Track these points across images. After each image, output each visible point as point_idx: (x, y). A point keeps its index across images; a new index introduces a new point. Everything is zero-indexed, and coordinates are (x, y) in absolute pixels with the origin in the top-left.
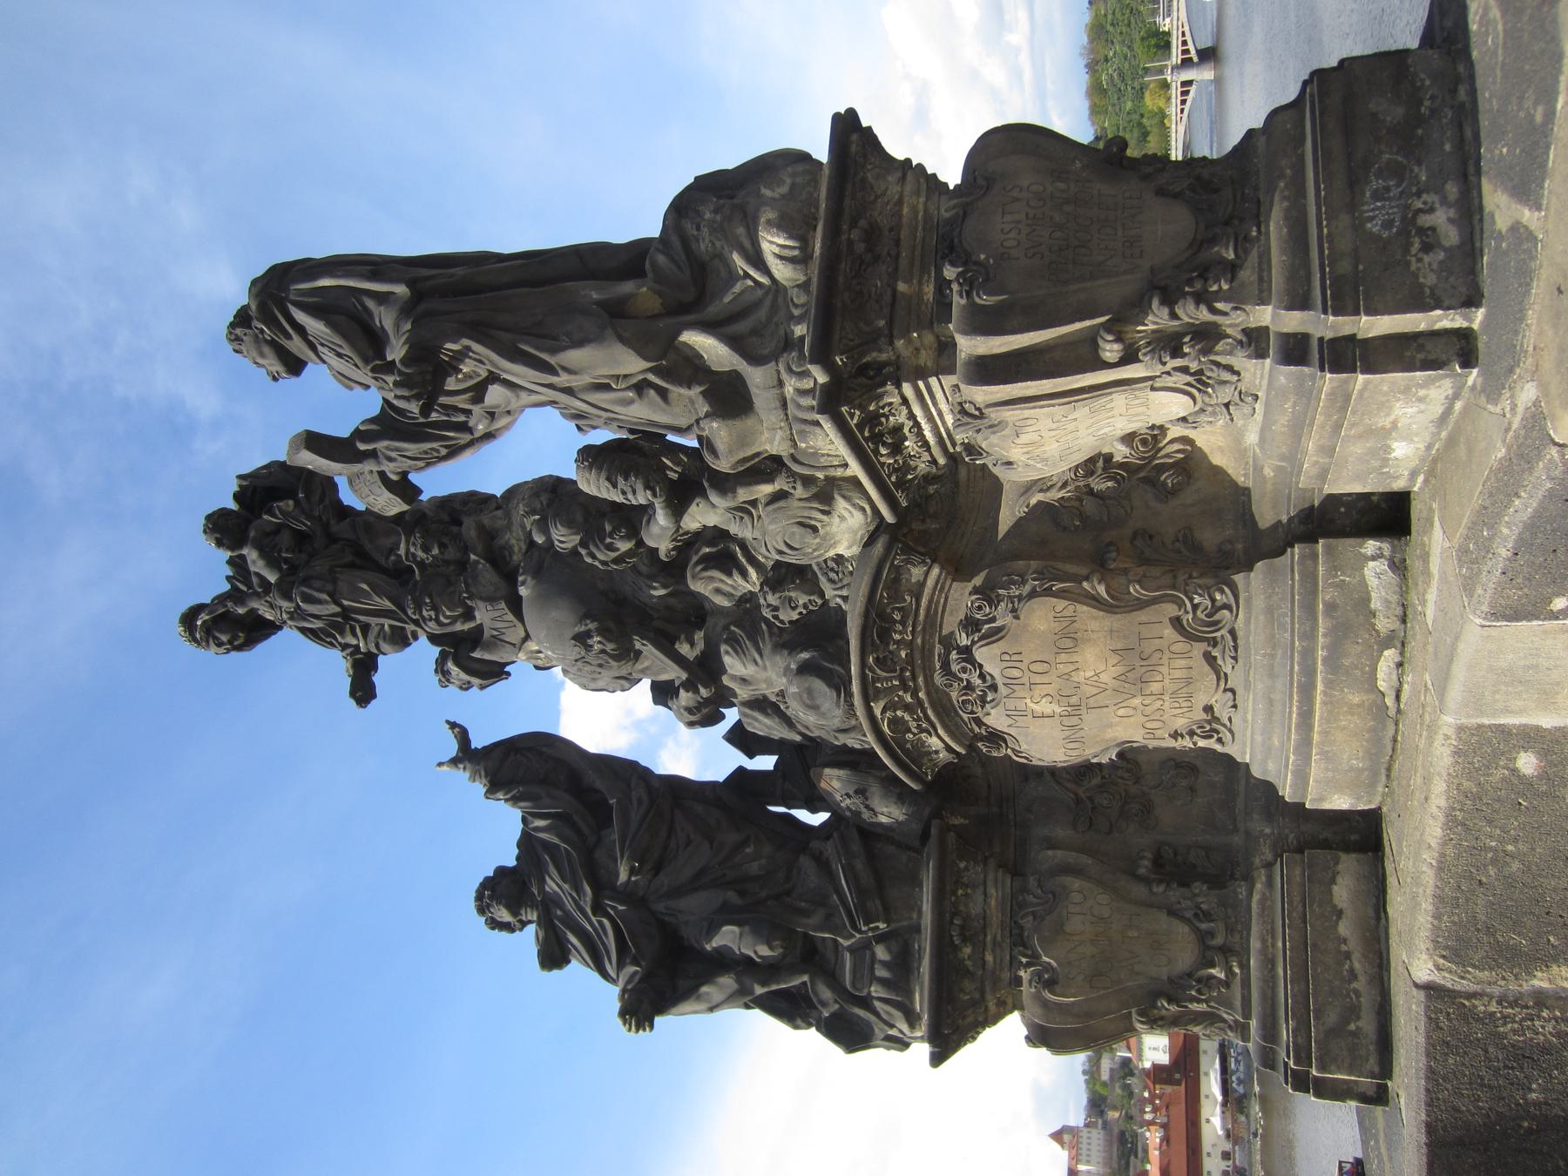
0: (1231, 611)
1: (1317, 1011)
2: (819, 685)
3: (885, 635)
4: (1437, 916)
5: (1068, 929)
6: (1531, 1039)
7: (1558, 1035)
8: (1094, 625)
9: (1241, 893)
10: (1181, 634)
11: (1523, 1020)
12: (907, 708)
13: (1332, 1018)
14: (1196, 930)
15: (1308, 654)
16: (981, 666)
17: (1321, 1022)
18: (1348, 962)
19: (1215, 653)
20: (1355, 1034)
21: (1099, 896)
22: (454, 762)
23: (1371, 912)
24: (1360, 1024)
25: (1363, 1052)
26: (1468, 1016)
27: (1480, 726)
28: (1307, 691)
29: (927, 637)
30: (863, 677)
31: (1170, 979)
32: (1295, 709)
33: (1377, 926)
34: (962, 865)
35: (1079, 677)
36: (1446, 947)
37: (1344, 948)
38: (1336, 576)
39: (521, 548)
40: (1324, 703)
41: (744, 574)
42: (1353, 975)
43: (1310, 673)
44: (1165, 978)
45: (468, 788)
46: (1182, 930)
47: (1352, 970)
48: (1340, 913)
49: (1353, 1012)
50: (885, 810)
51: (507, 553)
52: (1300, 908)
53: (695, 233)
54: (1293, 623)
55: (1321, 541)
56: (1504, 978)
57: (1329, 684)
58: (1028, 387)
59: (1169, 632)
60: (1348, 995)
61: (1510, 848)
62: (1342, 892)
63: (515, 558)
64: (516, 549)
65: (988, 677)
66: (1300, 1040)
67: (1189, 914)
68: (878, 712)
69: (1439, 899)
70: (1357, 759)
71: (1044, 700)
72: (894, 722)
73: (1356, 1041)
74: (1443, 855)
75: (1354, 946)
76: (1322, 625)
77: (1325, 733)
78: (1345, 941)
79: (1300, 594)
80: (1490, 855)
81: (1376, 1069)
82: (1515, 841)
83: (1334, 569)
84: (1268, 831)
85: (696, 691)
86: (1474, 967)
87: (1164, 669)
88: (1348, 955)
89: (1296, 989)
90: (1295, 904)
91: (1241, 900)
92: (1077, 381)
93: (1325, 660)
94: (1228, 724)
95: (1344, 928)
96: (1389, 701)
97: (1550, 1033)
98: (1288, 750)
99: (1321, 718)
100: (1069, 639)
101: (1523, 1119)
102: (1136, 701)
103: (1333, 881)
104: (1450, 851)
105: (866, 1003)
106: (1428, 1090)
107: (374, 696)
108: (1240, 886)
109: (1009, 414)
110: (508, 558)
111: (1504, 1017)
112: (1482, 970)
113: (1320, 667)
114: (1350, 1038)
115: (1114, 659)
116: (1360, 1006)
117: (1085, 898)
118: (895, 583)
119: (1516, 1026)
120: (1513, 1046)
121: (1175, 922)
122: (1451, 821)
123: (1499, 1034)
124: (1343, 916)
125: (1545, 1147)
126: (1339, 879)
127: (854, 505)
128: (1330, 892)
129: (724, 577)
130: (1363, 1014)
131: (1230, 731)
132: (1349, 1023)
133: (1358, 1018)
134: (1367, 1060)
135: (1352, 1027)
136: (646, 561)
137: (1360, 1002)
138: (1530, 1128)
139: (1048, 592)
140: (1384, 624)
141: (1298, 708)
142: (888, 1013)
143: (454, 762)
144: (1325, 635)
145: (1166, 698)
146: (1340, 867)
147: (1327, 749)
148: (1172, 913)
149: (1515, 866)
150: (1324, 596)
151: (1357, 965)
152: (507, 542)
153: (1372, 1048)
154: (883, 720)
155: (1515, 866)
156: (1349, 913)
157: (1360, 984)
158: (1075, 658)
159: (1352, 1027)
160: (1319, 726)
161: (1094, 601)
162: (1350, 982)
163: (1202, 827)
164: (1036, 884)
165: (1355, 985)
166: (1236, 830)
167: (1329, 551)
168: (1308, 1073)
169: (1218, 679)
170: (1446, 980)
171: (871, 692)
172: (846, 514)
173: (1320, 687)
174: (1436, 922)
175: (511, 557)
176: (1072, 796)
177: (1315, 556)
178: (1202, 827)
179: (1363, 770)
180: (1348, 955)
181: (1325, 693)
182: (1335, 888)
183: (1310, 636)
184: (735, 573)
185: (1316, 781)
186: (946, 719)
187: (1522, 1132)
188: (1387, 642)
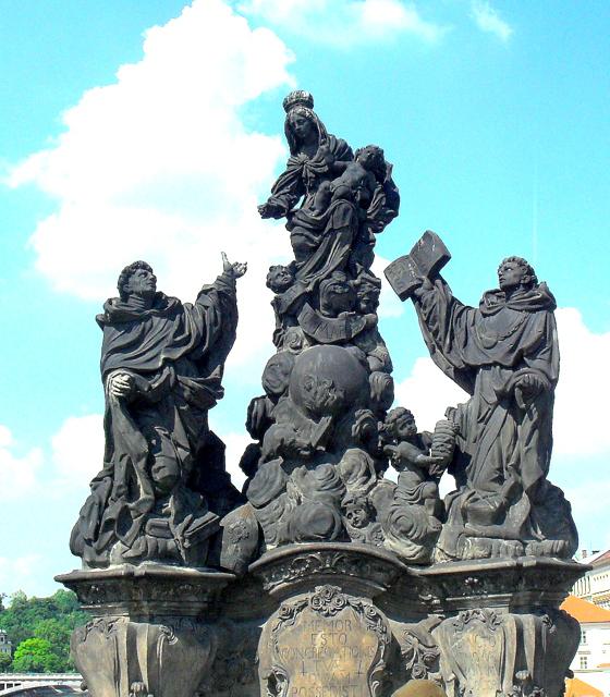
2: (327, 527)
3: (355, 562)
30: (336, 550)
35: (336, 657)
41: (364, 483)
45: (211, 274)
58: (512, 643)
85: (305, 449)
92: (511, 662)
100: (358, 655)
105: (142, 531)
109: (499, 637)
129: (362, 472)
139: (380, 644)
142: (139, 546)
158: (347, 657)
161: (373, 666)
172: (412, 548)
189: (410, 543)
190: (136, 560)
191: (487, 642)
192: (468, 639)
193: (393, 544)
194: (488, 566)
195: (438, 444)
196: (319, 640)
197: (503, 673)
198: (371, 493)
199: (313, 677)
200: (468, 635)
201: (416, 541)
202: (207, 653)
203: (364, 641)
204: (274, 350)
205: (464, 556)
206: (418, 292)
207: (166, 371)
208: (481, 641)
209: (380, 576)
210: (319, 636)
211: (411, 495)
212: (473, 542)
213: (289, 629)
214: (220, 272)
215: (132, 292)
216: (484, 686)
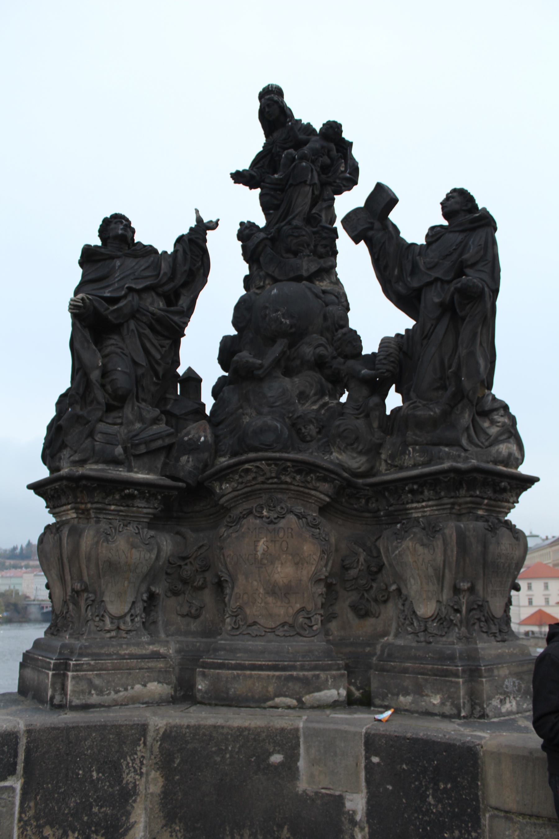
0: (308, 634)
1: (100, 674)
3: (299, 472)
4: (188, 727)
5: (134, 551)
6: (124, 772)
7: (127, 784)
8: (305, 572)
9: (144, 638)
10: (297, 611)
11: (134, 768)
12: (254, 478)
13: (97, 681)
14: (125, 615)
15: (294, 668)
16: (283, 518)
17: (95, 677)
18: (123, 690)
19: (286, 628)
20: (90, 693)
21: (146, 567)
22: (199, 220)
23: (146, 700)
24: (95, 696)
25: (81, 697)
26: (136, 743)
27: (298, 738)
28: (275, 668)
29: (293, 492)
31: (103, 601)
32: (264, 663)
33: (139, 703)
34: (159, 497)
36: (171, 732)
37: (129, 688)
38: (331, 678)
39: (322, 286)
40: (268, 676)
42: (117, 692)
43: (284, 669)
44: (104, 599)
46: (126, 609)
47: (119, 691)
48: (145, 685)
49: (100, 692)
50: (191, 459)
51: (320, 278)
52: (146, 667)
53: (500, 414)
54: (308, 661)
55: (346, 672)
56: (155, 758)
57: (279, 677)
59: (298, 606)
60: (108, 690)
61: (228, 756)
62: (154, 686)
63: (317, 283)
64: (321, 284)
65: (276, 521)
66: (85, 666)
67: (133, 611)
68: (258, 464)
69: (197, 728)
70: (235, 691)
71: (265, 547)
72: (247, 471)
73: (87, 694)
74: (223, 727)
75: (130, 692)
76: (309, 674)
77: (251, 676)
78: (132, 688)
79: (322, 664)
80: (224, 748)
81: (73, 704)
82: (231, 757)
83: (334, 677)
84: (171, 651)
86: (160, 745)
87: (279, 603)
88: (126, 689)
89: (109, 665)
90: (148, 664)
91: (141, 638)
93: (291, 676)
94: (245, 632)
95: (138, 687)
96: (270, 703)
97: (128, 780)
98: (236, 660)
99: (260, 675)
101: (84, 771)
102: (261, 591)
103: (159, 682)
104: (225, 731)
106: (95, 726)
107: (235, 182)
108: (147, 637)
110: (317, 279)
111: (134, 759)
112: (159, 748)
113: (288, 673)
114: (87, 691)
115: (285, 581)
116: (103, 695)
117: (147, 560)
118: (324, 479)
119: (130, 765)
120: (121, 764)
121: (130, 606)
122: (241, 730)
123: (126, 757)
124: (143, 687)
125: (70, 782)
126: (160, 685)
127: (363, 464)
128: (154, 681)
130: (99, 697)
131: (240, 634)
132: (95, 690)
133: (97, 695)
134: (78, 699)
135: (93, 692)
136: (321, 352)
137: (105, 695)
138: (79, 774)
140: (306, 699)
141: (264, 665)
143: (199, 220)
144: (304, 675)
145: (263, 605)
146: (165, 685)
147: (241, 678)
148: (134, 603)
149: (218, 759)
150: (323, 675)
151: (121, 694)
152: (325, 280)
153: (84, 701)
154: (251, 466)
155: (218, 759)
156: (145, 690)
157: (113, 696)
159: (93, 692)
160: (255, 674)
162: (114, 690)
163: (165, 620)
164: (152, 535)
165: (113, 693)
166: (167, 636)
167: (342, 675)
168: (69, 671)
169: (272, 629)
170: (151, 734)
171: (270, 462)
172: (358, 460)
173: (277, 673)
174: (185, 726)
175: (318, 280)
176: (190, 556)
177: (339, 669)
178: (165, 620)
179: (227, 693)
180: (126, 689)
181: (273, 676)
182: (156, 683)
183: (302, 668)
184: (316, 397)
185: (218, 673)
186: (243, 496)
187: (77, 771)
188: (299, 701)
189: (355, 455)
190: (82, 462)
191: (426, 551)
192: (408, 548)
193: (340, 457)
194: (427, 470)
195: (381, 357)
196: (262, 546)
197: (443, 583)
198: (323, 412)
199: (255, 583)
200: (408, 543)
201: (360, 453)
202: (153, 556)
203: (305, 548)
204: (244, 292)
205: (406, 464)
206: (370, 233)
207: (129, 298)
208: (420, 549)
209: (325, 487)
210: (261, 543)
211: (358, 410)
212: (414, 450)
213: (234, 535)
214: (193, 224)
215: (109, 238)
216: (424, 596)
